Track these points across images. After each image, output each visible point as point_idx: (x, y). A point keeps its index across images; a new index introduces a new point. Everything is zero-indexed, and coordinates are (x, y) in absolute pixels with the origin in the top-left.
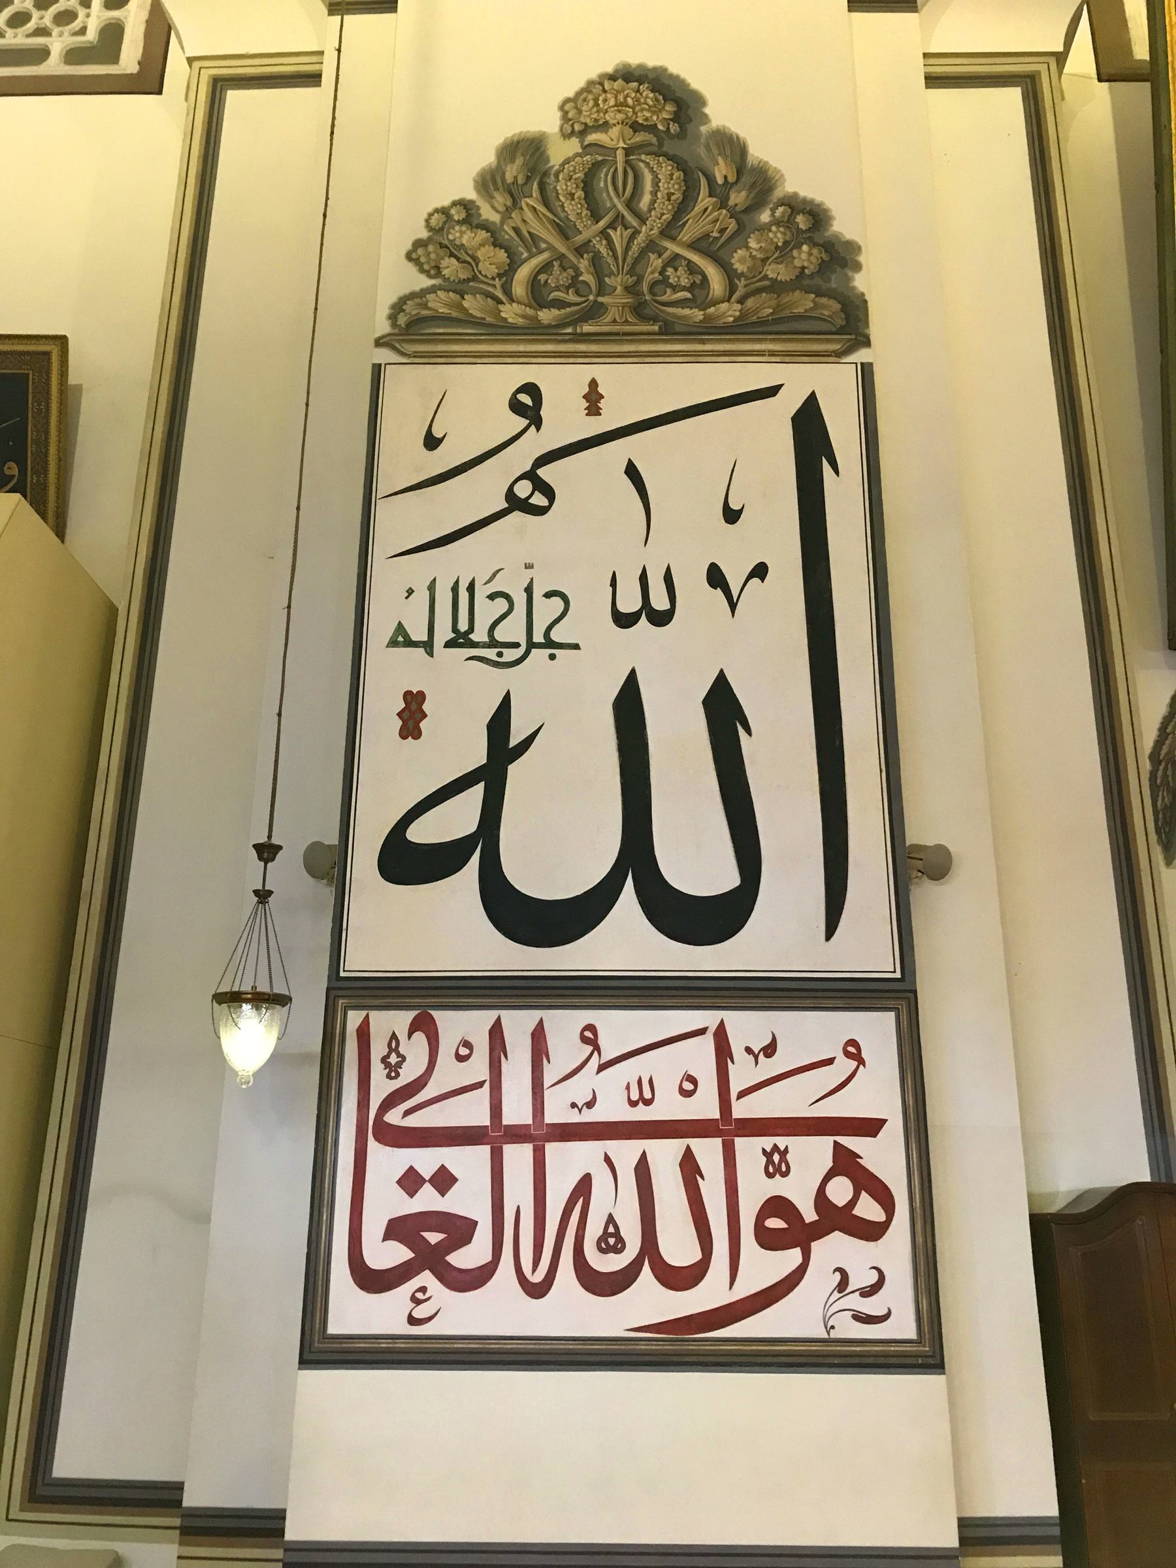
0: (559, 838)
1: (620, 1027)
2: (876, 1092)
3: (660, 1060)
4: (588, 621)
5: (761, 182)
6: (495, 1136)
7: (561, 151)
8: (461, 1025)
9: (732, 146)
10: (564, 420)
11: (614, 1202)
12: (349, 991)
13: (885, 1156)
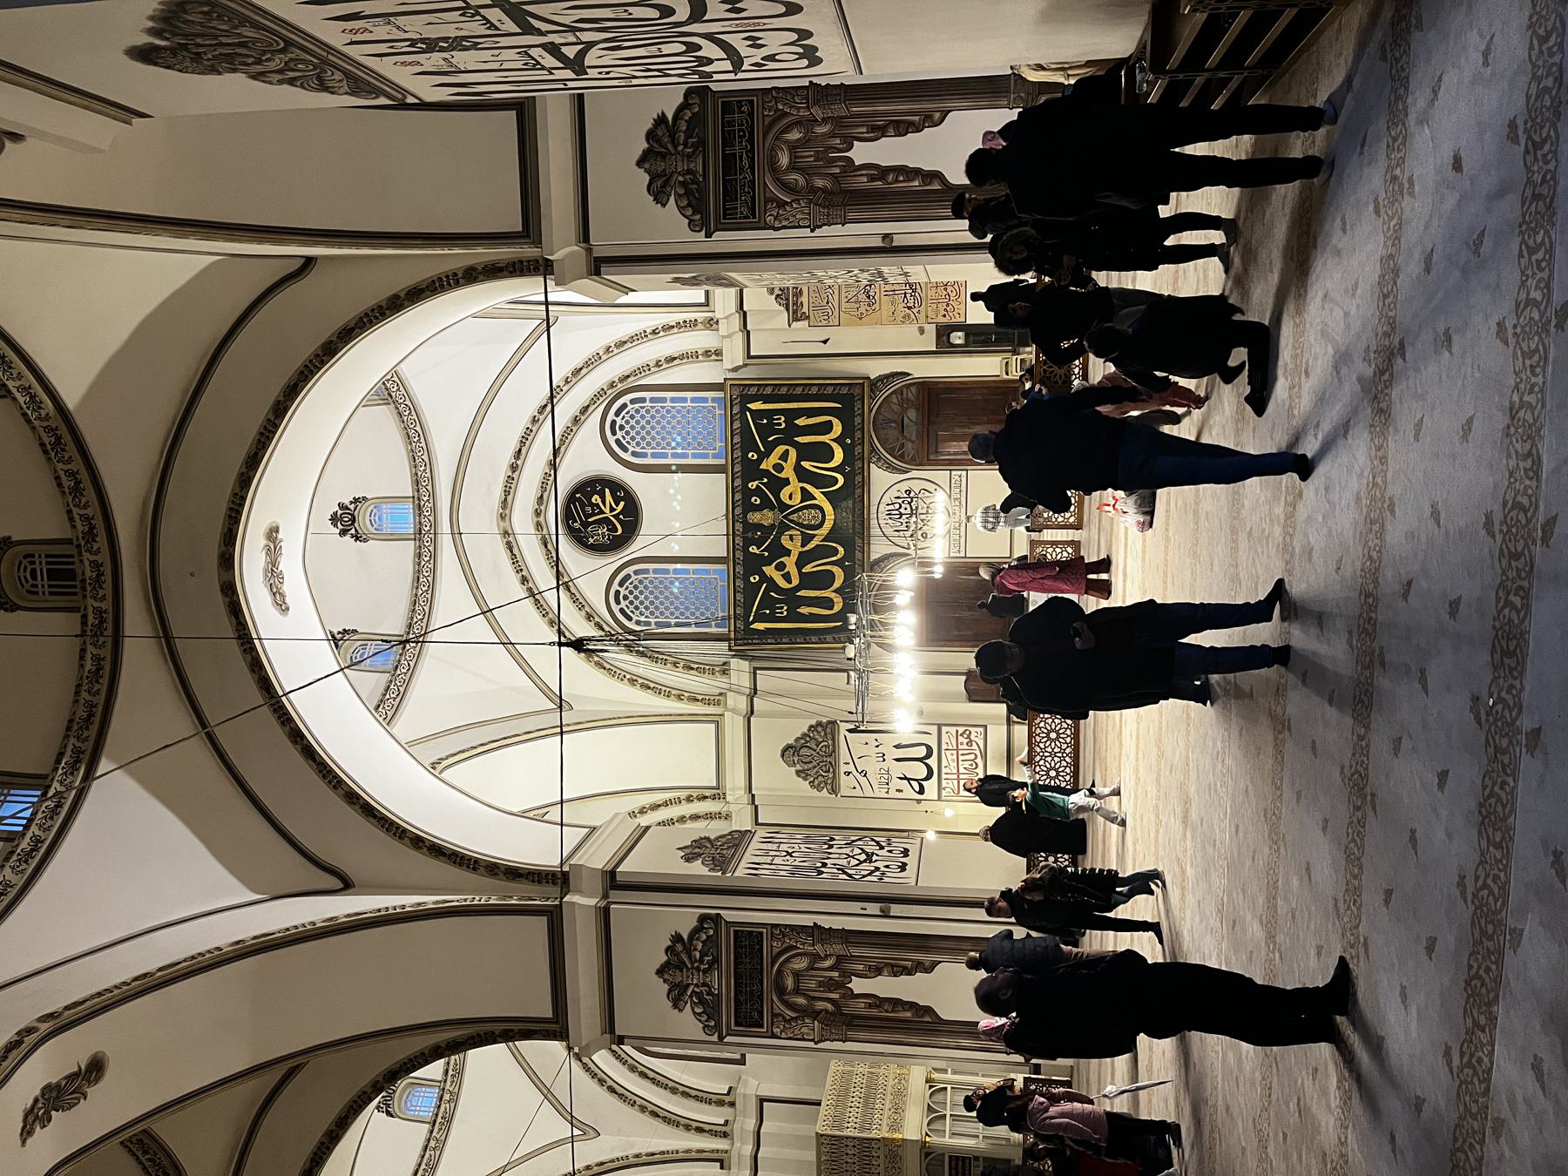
0: (920, 771)
1: (944, 763)
2: (953, 730)
3: (949, 758)
4: (885, 765)
5: (805, 735)
6: (959, 779)
7: (798, 767)
8: (944, 784)
9: (797, 740)
10: (851, 768)
11: (967, 764)
12: (939, 799)
13: (961, 730)
